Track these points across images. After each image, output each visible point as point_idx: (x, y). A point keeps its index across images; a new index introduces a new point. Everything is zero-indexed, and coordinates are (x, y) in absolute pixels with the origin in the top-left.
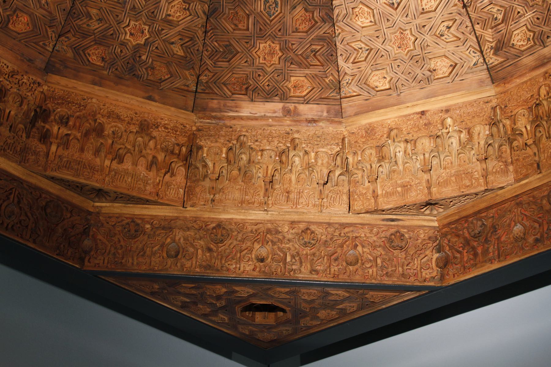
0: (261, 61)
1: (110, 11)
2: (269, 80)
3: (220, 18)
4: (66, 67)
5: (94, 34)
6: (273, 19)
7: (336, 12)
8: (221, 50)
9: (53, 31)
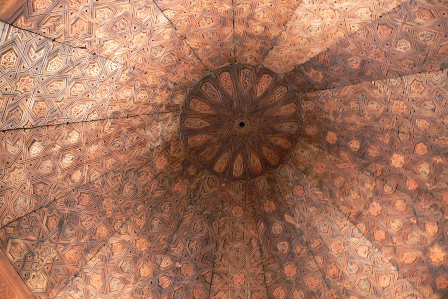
6: (434, 32)
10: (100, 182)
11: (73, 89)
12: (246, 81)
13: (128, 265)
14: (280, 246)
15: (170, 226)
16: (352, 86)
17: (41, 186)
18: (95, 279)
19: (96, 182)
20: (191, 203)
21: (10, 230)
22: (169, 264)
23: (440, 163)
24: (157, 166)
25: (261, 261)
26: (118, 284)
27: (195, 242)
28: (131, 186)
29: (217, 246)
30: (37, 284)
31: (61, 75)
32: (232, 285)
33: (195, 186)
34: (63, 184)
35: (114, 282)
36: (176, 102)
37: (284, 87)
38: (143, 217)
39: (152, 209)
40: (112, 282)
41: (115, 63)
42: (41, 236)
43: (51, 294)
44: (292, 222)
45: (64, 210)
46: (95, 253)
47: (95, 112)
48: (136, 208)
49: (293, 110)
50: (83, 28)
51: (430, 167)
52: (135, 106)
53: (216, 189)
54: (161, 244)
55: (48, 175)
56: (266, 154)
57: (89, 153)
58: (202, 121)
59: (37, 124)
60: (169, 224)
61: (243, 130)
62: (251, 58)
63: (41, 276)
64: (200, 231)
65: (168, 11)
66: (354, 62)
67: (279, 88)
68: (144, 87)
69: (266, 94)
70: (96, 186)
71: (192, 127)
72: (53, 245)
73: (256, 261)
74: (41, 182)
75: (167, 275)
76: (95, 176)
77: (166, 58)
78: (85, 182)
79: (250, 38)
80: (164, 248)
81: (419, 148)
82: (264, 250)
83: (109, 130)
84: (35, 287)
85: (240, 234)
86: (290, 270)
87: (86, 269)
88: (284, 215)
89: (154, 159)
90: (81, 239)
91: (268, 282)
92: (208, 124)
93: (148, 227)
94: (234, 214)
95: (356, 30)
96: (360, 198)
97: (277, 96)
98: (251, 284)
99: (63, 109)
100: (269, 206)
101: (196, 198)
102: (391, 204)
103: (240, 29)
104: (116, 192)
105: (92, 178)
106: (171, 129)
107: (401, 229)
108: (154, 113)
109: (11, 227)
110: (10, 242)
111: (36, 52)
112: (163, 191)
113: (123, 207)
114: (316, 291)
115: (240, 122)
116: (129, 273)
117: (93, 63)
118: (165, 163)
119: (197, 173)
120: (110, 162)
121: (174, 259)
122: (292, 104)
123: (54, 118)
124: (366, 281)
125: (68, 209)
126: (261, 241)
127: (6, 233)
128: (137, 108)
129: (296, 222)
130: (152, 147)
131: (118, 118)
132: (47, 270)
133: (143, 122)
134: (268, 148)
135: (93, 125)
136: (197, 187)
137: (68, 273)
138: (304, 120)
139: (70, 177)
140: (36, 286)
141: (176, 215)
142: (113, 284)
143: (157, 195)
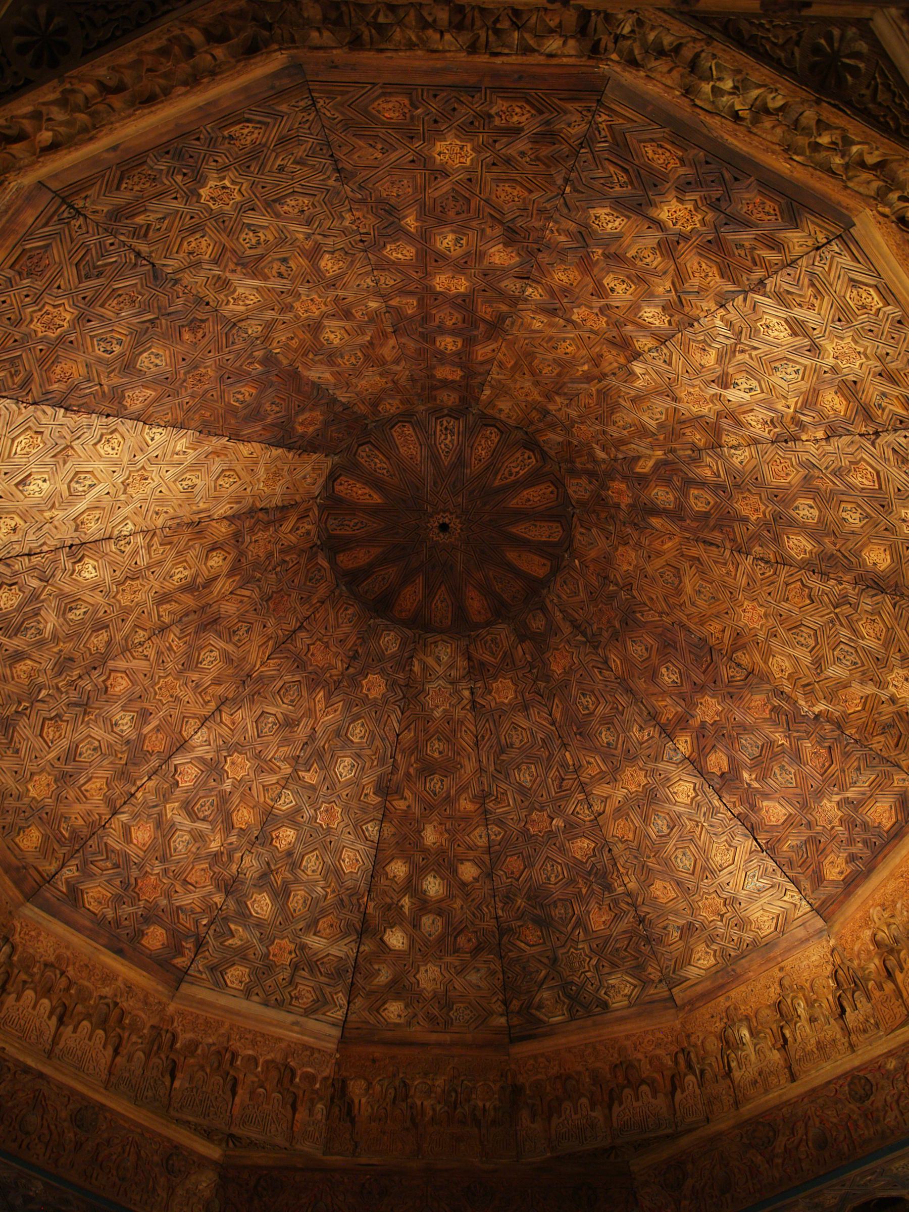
0: (47, 307)
1: (279, 185)
2: (12, 305)
3: (141, 279)
4: (273, 88)
5: (273, 151)
7: (49, 410)
8: (99, 263)
9: (335, 119)
10: (496, 829)
11: (309, 872)
12: (352, 523)
13: (660, 822)
14: (700, 507)
15: (620, 708)
16: (306, 373)
17: (462, 940)
18: (658, 893)
19: (493, 837)
20: (596, 648)
21: (515, 1005)
22: (688, 739)
23: (417, 220)
24: (506, 701)
25: (728, 553)
26: (684, 854)
27: (664, 670)
28: (524, 767)
29: (682, 626)
30: (622, 993)
31: (281, 894)
32: (762, 636)
33: (568, 623)
34: (473, 900)
35: (679, 860)
36: (394, 649)
37: (359, 451)
38: (587, 759)
39: (580, 734)
40: (676, 864)
41: (280, 798)
42: (545, 961)
43: (651, 977)
44: (651, 463)
45: (519, 908)
46: (616, 873)
47: (364, 827)
48: (568, 765)
49: (409, 430)
50: (202, 870)
51: (440, 234)
52: (378, 742)
53: (581, 582)
54: (647, 740)
55: (448, 923)
56: (512, 478)
57: (434, 844)
58: (437, 597)
59: (356, 929)
60: (617, 709)
61: (456, 524)
62: (297, 529)
63: (610, 982)
64: (647, 649)
65: (184, 734)
66: (240, 396)
67: (362, 461)
68: (340, 733)
69: (376, 483)
70: (499, 838)
71: (450, 615)
72: (569, 944)
73: (725, 564)
74: (455, 938)
75: (707, 750)
76: (481, 837)
77: (285, 701)
78: (486, 858)
79: (243, 560)
80: (657, 735)
81: (400, 256)
82: (709, 536)
83: (405, 799)
84: (626, 998)
85: (667, 573)
86: (751, 508)
87: (637, 900)
88: (637, 473)
89: (493, 704)
90: (580, 892)
91: (771, 556)
92: (443, 588)
93: (607, 753)
94: (631, 568)
95: (160, 430)
96: (573, 339)
97: (379, 465)
98: (769, 594)
99: (341, 887)
100: (620, 493)
101: (589, 631)
102: (566, 291)
103: (222, 586)
104: (522, 802)
105: (482, 842)
106: (446, 658)
107: (628, 277)
108: (404, 697)
109: (511, 1002)
110: (533, 1011)
111: (234, 936)
112: (556, 700)
113: (556, 793)
114: (803, 472)
115: (437, 531)
116: (674, 827)
117: (272, 839)
118: (508, 682)
119: (544, 609)
120: (465, 805)
121: (682, 722)
122: (394, 434)
123: (355, 901)
124: (777, 364)
125: (520, 901)
126: (687, 535)
127: (518, 1012)
128: (383, 740)
129: (650, 457)
130: (468, 707)
131: (390, 780)
132: (606, 970)
133: (412, 726)
134: (496, 474)
135: (388, 830)
136: (570, 621)
137: (631, 934)
138: (430, 405)
139: (464, 884)
140: (626, 995)
141: (606, 686)
142: (681, 865)
143: (558, 715)
